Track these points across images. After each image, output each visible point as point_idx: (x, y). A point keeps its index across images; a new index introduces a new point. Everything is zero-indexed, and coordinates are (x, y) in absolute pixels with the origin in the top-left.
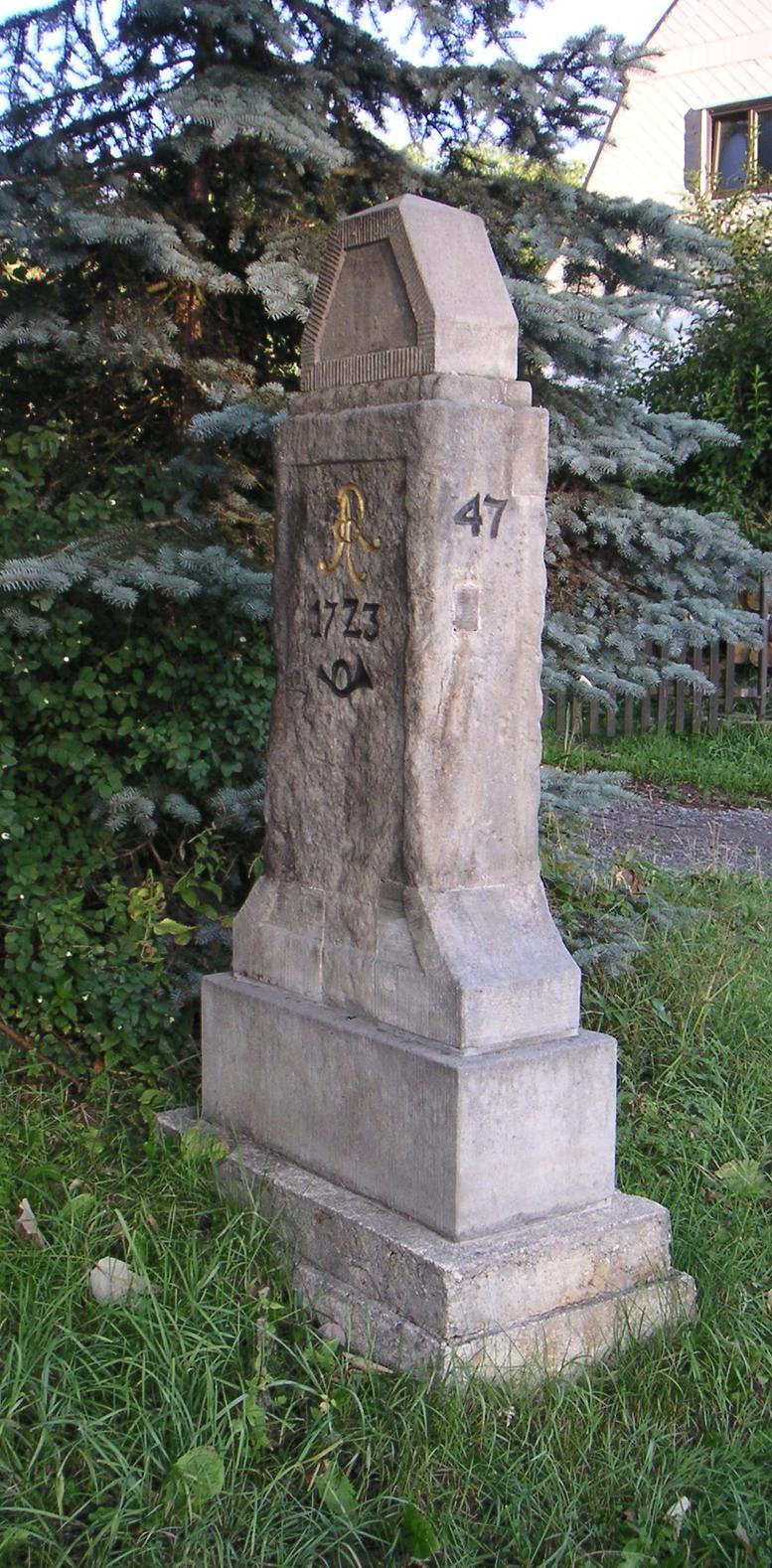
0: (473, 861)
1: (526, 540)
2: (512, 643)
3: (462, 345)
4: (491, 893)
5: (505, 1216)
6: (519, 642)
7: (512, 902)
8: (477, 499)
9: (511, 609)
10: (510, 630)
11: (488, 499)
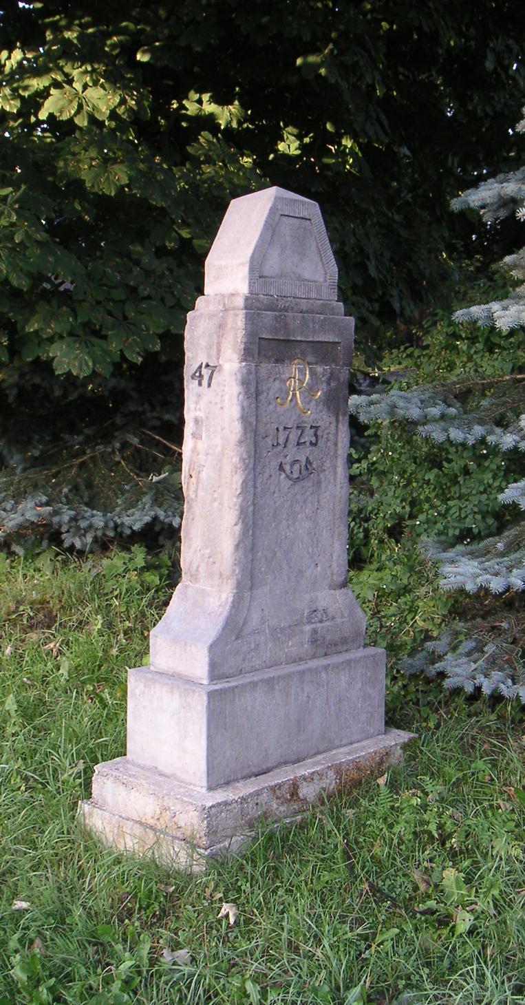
0: (197, 570)
1: (226, 389)
2: (219, 449)
3: (218, 278)
4: (203, 592)
5: (148, 763)
6: (223, 449)
7: (211, 599)
8: (200, 367)
9: (219, 429)
10: (218, 441)
11: (207, 366)
